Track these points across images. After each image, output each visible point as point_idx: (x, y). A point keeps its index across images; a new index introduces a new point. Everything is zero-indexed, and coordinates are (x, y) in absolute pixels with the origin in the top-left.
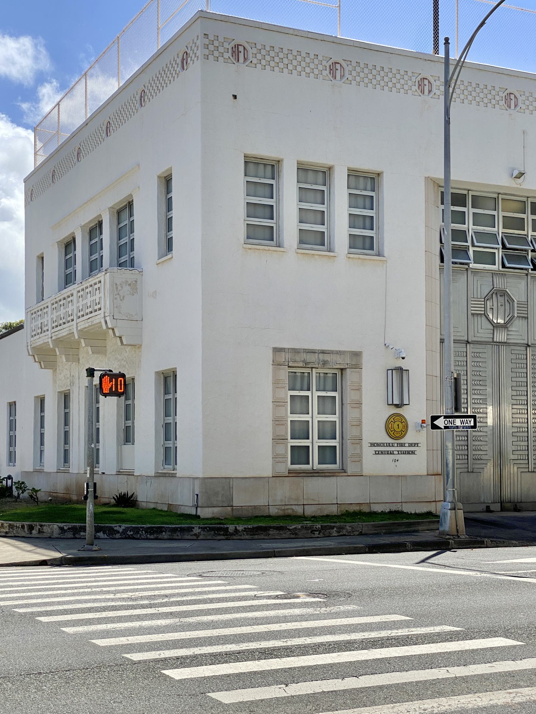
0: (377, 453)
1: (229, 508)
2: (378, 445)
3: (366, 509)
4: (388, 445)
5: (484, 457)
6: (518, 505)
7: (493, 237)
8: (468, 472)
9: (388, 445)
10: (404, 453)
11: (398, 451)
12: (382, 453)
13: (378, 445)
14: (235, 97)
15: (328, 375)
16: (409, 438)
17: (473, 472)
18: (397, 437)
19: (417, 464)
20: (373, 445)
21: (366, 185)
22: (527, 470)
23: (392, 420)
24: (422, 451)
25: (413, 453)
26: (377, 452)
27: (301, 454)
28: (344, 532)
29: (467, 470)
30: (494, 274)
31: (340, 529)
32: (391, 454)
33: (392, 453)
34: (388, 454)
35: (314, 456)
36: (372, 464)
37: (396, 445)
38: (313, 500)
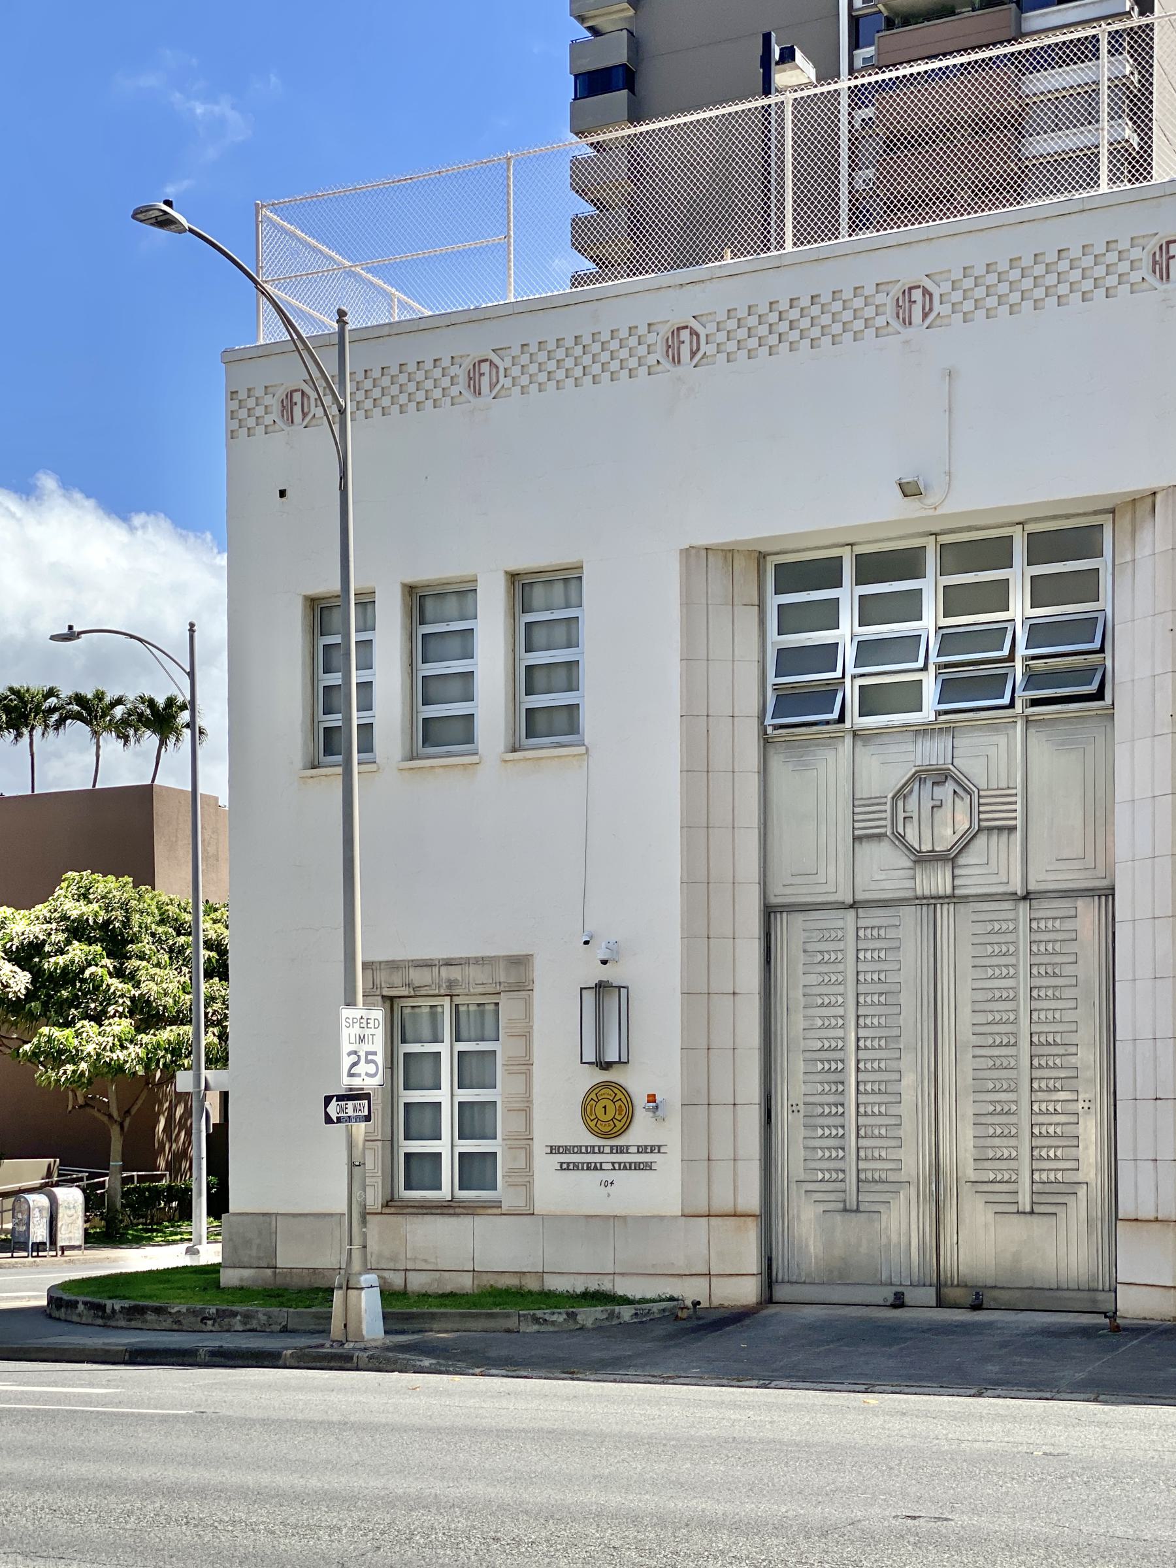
0: (565, 1167)
1: (269, 1272)
2: (568, 1150)
3: (532, 1285)
4: (591, 1150)
5: (892, 1177)
8: (845, 1210)
9: (591, 1150)
10: (625, 1168)
11: (613, 1163)
12: (576, 1167)
13: (568, 1150)
14: (282, 494)
15: (487, 1007)
16: (636, 1136)
17: (857, 1211)
18: (606, 1133)
19: (659, 1191)
20: (554, 1150)
21: (543, 597)
22: (1013, 1208)
23: (593, 1096)
24: (670, 1165)
25: (648, 1166)
26: (565, 1166)
27: (421, 1169)
28: (254, 1324)
31: (247, 1317)
32: (596, 1168)
33: (598, 1167)
34: (588, 1169)
35: (448, 1171)
36: (556, 1190)
37: (607, 1150)
38: (425, 1261)
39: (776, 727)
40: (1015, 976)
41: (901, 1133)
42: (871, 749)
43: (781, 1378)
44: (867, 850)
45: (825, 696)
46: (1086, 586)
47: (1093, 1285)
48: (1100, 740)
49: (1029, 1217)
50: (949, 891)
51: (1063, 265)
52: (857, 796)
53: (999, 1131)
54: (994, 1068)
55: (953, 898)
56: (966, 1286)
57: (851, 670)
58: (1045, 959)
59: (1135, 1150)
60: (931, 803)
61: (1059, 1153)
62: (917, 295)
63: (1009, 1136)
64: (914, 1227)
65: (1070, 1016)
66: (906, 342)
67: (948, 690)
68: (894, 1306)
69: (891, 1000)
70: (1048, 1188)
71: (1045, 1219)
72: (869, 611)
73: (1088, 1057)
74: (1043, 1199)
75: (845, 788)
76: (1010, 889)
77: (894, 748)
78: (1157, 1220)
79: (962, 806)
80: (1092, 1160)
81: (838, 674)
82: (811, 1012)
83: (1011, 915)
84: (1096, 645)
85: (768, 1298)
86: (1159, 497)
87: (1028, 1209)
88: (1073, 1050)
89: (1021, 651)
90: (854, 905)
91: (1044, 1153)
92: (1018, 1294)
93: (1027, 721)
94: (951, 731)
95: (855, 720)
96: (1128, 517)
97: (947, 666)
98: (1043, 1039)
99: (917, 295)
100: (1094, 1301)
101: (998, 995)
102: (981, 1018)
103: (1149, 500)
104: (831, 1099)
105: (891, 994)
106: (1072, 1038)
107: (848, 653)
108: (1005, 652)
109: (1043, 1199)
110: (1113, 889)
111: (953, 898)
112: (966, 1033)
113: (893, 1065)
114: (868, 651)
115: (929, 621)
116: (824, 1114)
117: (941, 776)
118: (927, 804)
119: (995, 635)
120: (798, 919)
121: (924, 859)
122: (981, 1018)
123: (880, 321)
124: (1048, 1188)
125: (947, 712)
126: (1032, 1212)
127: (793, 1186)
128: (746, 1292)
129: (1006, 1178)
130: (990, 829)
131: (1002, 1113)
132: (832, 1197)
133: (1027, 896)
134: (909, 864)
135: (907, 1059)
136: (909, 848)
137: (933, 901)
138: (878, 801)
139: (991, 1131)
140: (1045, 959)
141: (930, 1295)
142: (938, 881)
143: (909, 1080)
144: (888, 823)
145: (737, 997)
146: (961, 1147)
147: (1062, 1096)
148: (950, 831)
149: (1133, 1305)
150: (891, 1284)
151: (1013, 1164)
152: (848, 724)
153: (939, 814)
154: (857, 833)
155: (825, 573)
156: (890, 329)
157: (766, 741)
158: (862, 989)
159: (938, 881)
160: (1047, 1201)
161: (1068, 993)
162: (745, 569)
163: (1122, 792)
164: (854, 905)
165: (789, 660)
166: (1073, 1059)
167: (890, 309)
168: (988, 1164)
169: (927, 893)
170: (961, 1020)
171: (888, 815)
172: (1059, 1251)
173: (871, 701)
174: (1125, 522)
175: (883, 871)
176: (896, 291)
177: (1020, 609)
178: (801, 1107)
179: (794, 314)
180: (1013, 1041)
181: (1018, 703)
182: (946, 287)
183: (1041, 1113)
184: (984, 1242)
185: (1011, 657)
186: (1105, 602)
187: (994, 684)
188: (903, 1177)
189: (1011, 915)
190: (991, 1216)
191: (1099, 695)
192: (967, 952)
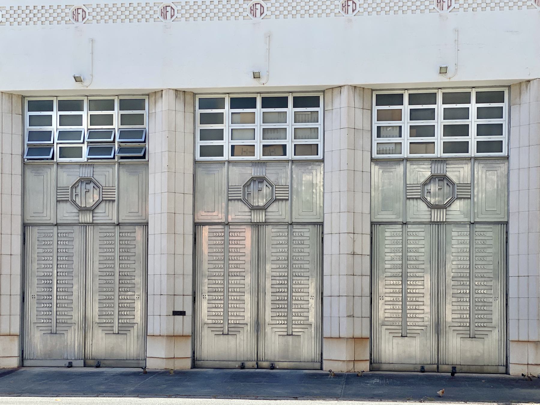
6: (102, 362)
7: (77, 135)
29: (50, 331)
30: (81, 165)
39: (28, 159)
40: (114, 252)
41: (73, 306)
42: (64, 170)
43: (25, 393)
44: (61, 205)
45: (47, 149)
46: (140, 119)
47: (138, 358)
48: (144, 172)
49: (117, 335)
50: (91, 221)
51: (131, 9)
52: (59, 186)
53: (107, 305)
54: (106, 283)
55: (92, 224)
56: (94, 359)
57: (56, 141)
58: (124, 246)
59: (153, 313)
60: (85, 190)
61: (128, 313)
62: (80, 11)
63: (111, 307)
64: (76, 339)
65: (133, 266)
66: (76, 27)
67: (92, 151)
68: (68, 367)
69: (70, 258)
70: (124, 325)
71: (123, 335)
72: (63, 120)
73: (138, 280)
74: (123, 329)
75: (54, 183)
76: (112, 222)
77: (72, 170)
78: (160, 336)
79: (96, 192)
80: (139, 315)
81: (52, 142)
82: (40, 262)
83: (113, 231)
84: (143, 140)
85: (22, 365)
86: (164, 92)
87: (117, 332)
88: (133, 278)
89: (117, 140)
90: (57, 225)
91: (123, 313)
92: (112, 362)
93: (119, 164)
94: (92, 165)
95: (57, 159)
96: (154, 97)
97: (91, 143)
98: (123, 274)
99: (80, 11)
100: (139, 363)
101: (108, 258)
102: (102, 266)
103: (160, 93)
104: (47, 293)
105: (70, 257)
106: (134, 274)
107: (56, 135)
108: (112, 140)
109: (123, 329)
110: (148, 223)
111: (92, 224)
112: (97, 271)
113: (70, 282)
114: (62, 135)
115: (85, 126)
116: (45, 299)
117: (89, 181)
118: (84, 191)
119: (108, 133)
120: (36, 229)
121: (82, 210)
122: (102, 266)
123: (67, 19)
124: (124, 325)
125: (91, 159)
126: (118, 333)
127: (32, 325)
128: (14, 363)
129: (110, 321)
130: (106, 200)
131: (109, 299)
132: (46, 328)
133: (118, 225)
134: (77, 211)
135: (75, 280)
136: (77, 206)
137: (86, 225)
138: (66, 188)
139: (105, 305)
140: (124, 246)
141: (81, 363)
142: (88, 218)
143: (75, 287)
144: (69, 196)
145: (12, 256)
146: (94, 310)
147: (129, 293)
148: (92, 201)
149: (152, 365)
150: (67, 359)
151: (112, 317)
152: (55, 160)
153: (88, 194)
154: (58, 199)
155: (47, 106)
156: (70, 22)
157: (24, 164)
158: (59, 254)
159: (88, 218)
160: (124, 329)
161: (132, 258)
162: (17, 103)
163: (151, 191)
164: (57, 225)
165: (32, 135)
166: (133, 281)
167: (71, 15)
168: (104, 317)
169: (83, 221)
170: (94, 266)
171: (70, 193)
172: (128, 347)
173: (63, 152)
174: (152, 99)
175: (67, 213)
176: (73, 9)
177: (116, 125)
178: (36, 296)
179: (35, 11)
180: (113, 274)
181: (116, 158)
182: (91, 10)
183: (122, 299)
184: (101, 344)
185: (114, 142)
186: (145, 125)
187: (108, 150)
188: (73, 321)
189: (113, 231)
190: (104, 335)
191: (144, 157)
192: (97, 243)
